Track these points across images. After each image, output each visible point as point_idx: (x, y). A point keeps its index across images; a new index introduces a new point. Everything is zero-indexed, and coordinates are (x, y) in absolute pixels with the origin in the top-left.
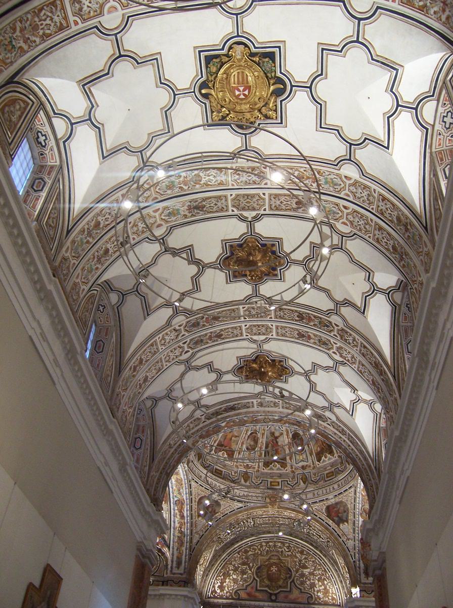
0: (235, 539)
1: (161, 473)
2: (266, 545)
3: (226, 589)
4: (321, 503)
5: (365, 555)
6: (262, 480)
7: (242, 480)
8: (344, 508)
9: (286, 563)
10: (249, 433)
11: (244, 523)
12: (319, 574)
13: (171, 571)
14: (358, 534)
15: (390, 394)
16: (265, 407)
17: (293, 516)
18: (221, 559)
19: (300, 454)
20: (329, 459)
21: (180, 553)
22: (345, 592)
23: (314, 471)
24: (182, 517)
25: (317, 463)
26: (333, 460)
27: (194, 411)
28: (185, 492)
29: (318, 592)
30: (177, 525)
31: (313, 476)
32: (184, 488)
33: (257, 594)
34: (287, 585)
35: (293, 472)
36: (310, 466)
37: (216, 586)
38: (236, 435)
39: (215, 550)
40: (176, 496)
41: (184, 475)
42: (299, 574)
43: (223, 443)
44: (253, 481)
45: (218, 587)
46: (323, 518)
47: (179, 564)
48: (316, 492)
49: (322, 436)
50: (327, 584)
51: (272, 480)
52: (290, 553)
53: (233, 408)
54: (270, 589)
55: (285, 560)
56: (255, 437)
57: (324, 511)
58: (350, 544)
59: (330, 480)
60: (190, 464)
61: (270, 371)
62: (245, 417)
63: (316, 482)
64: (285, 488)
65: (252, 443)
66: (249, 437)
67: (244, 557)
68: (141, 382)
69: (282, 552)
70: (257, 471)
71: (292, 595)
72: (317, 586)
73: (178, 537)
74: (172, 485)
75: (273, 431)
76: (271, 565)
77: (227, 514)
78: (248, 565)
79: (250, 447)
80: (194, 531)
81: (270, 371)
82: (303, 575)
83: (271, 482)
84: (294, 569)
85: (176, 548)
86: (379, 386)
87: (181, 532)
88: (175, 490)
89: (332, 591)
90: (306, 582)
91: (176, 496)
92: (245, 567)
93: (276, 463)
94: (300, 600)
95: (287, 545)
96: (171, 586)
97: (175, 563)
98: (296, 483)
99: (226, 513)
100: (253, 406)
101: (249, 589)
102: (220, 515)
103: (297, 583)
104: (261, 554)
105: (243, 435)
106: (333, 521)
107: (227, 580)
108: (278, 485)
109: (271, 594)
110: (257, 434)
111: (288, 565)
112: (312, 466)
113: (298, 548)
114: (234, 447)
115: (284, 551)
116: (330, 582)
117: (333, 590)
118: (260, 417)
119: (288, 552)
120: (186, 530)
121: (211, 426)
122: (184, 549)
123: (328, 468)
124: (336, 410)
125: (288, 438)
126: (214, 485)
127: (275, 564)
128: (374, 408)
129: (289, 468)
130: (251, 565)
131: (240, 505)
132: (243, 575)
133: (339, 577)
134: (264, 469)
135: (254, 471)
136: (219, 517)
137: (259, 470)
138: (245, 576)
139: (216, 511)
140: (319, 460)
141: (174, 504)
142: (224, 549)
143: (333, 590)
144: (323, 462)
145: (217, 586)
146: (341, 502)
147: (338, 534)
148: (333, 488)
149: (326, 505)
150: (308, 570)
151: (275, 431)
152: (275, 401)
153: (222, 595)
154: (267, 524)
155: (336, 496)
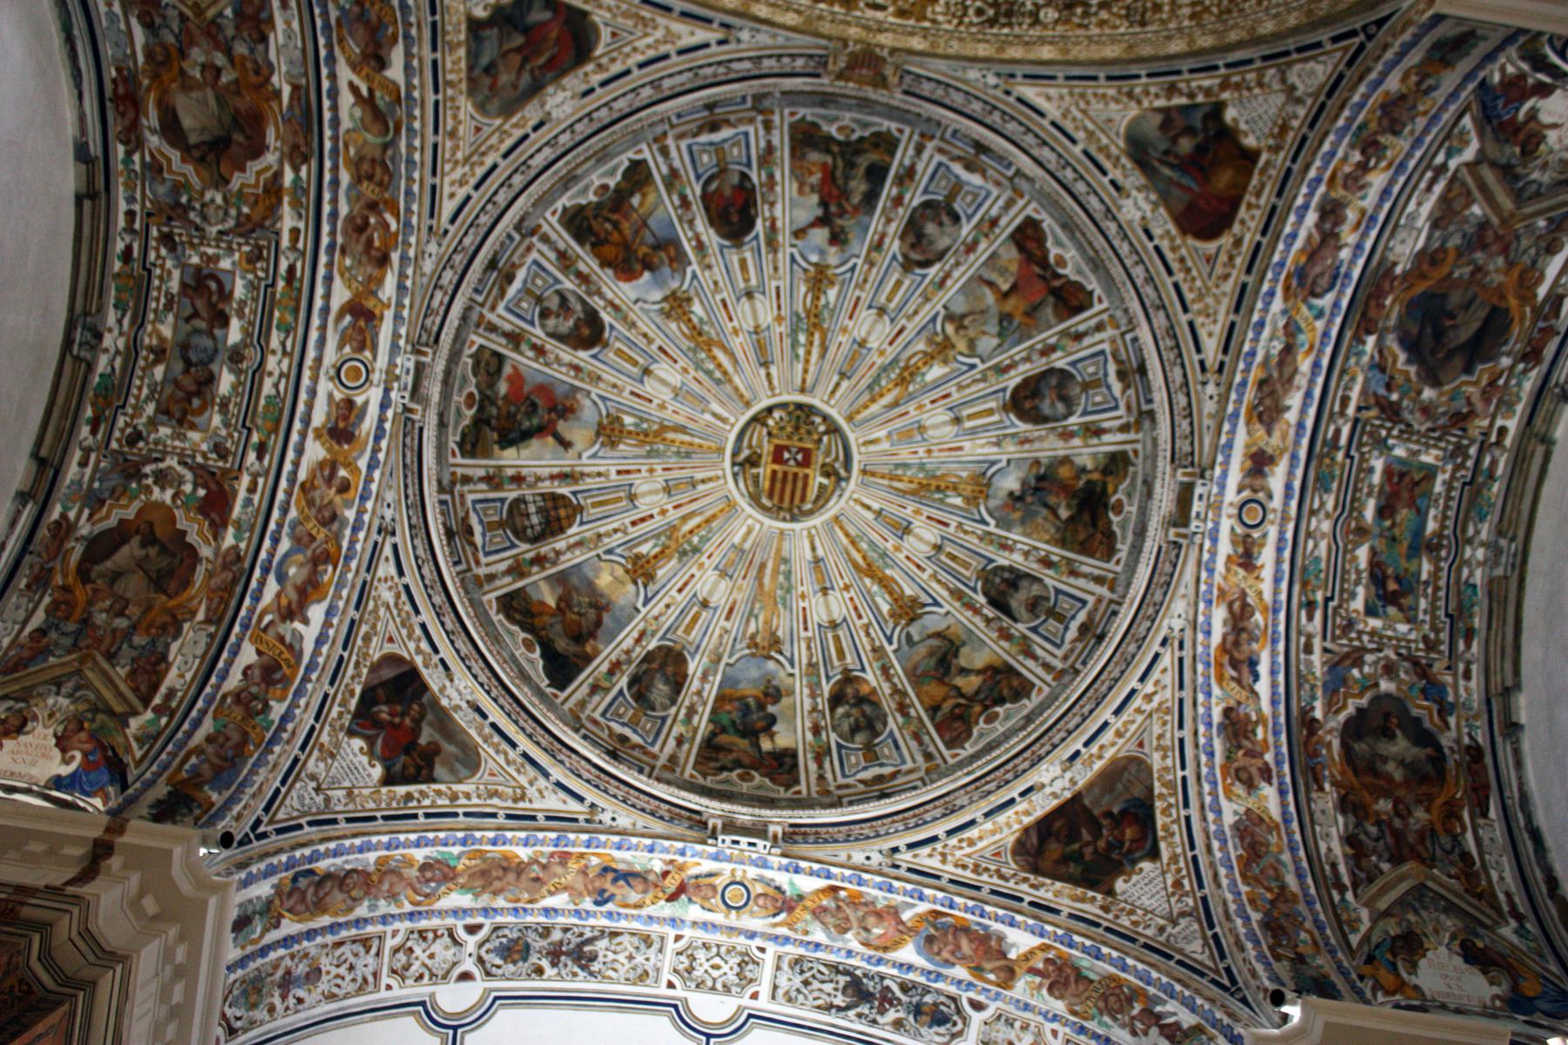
4: (617, 68)
8: (492, 87)
24: (1331, 212)
25: (647, 155)
30: (1377, 180)
32: (1259, 358)
35: (761, 112)
38: (987, 291)
41: (1229, 445)
43: (1051, 300)
56: (913, 246)
57: (605, 35)
62: (818, 946)
65: (930, 228)
66: (941, 256)
74: (1312, 382)
75: (833, 250)
77: (1109, 78)
79: (945, 219)
80: (1302, 112)
87: (1370, 147)
88: (1311, 347)
91: (1320, 314)
93: (840, 137)
105: (961, 276)
110: (905, 256)
114: (1011, 255)
120: (1339, 150)
125: (773, 220)
131: (1030, 92)
137: (922, 135)
139: (1157, 119)
141: (1347, 276)
146: (508, 110)
149: (590, 67)
151: (825, 246)
155: (536, 129)
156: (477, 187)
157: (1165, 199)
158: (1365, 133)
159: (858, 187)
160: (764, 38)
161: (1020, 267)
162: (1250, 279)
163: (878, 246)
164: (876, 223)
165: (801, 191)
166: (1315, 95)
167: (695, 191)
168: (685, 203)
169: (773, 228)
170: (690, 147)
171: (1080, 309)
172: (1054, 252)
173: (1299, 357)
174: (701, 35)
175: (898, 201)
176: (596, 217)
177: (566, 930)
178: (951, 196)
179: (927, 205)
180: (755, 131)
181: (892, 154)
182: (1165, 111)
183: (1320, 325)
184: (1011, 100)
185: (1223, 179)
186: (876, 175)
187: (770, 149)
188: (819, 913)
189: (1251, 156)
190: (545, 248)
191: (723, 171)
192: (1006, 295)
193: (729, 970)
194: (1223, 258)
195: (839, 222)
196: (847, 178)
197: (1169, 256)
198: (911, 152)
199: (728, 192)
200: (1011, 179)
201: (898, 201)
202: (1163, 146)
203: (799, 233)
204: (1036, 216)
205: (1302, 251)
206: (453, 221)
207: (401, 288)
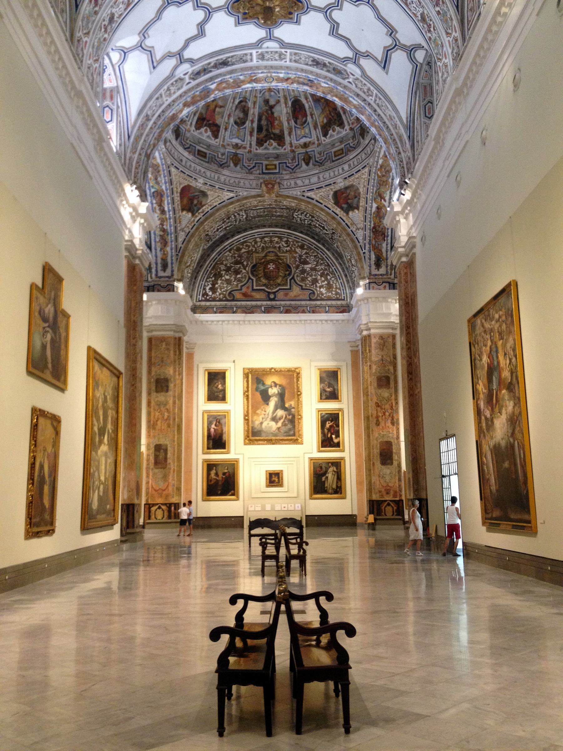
0: (225, 235)
1: (140, 154)
2: (261, 241)
3: (219, 290)
4: (328, 189)
5: (377, 245)
6: (256, 163)
7: (232, 165)
8: (355, 193)
9: (285, 260)
10: (237, 101)
11: (235, 216)
12: (322, 269)
13: (156, 275)
14: (370, 222)
15: (447, 33)
16: (268, 60)
17: (293, 205)
18: (210, 259)
19: (302, 127)
20: (339, 133)
21: (164, 254)
22: (350, 286)
23: (319, 149)
24: (163, 212)
25: (323, 138)
26: (344, 133)
27: (176, 68)
28: (163, 181)
29: (320, 287)
31: (317, 155)
32: (162, 176)
33: (254, 294)
34: (287, 283)
36: (314, 143)
37: (208, 288)
39: (204, 249)
40: (152, 187)
41: (161, 159)
42: (300, 271)
43: (204, 116)
44: (244, 164)
45: (210, 289)
46: (329, 206)
47: (165, 267)
48: (321, 176)
49: (340, 99)
50: (331, 279)
51: (267, 163)
52: (288, 248)
53: (225, 63)
54: (267, 287)
55: (284, 256)
56: (245, 106)
58: (360, 234)
59: (339, 159)
60: (168, 144)
61: (278, 5)
62: (241, 75)
63: (320, 164)
64: (284, 172)
65: (241, 115)
66: (237, 107)
67: (236, 255)
68: (106, 23)
69: (279, 247)
70: (248, 152)
71: (292, 293)
72: (320, 282)
73: (160, 236)
75: (267, 97)
76: (269, 262)
77: (216, 206)
78: (242, 263)
79: (238, 121)
80: (179, 228)
81: (278, 5)
82: (303, 271)
83: (266, 165)
84: (294, 265)
85: (158, 249)
86: (431, 23)
89: (336, 285)
90: (307, 278)
91: (152, 187)
92: (238, 266)
93: (271, 141)
94: (301, 297)
95: (285, 239)
96: (159, 291)
97: (159, 266)
98: (297, 166)
99: (215, 204)
100: (251, 60)
101: (244, 289)
102: (208, 208)
103: (298, 279)
104: (256, 252)
106: (342, 208)
107: (219, 282)
108: (275, 168)
109: (269, 293)
110: (246, 102)
111: (287, 261)
112: (316, 142)
113: (297, 242)
114: (219, 121)
115: (281, 246)
116: (333, 277)
117: (337, 284)
118: (261, 75)
119: (287, 247)
121: (198, 89)
122: (168, 249)
123: (336, 145)
124: (363, 62)
126: (198, 171)
127: (272, 261)
128: (415, 58)
129: (288, 147)
130: (245, 263)
131: (232, 195)
132: (237, 274)
133: (344, 271)
134: (256, 149)
135: (245, 152)
136: (207, 210)
138: (239, 276)
139: (203, 204)
140: (325, 135)
141: (151, 197)
142: (212, 248)
143: (337, 284)
144: (330, 137)
145: (208, 288)
146: (352, 186)
147: (346, 224)
148: (343, 169)
149: (334, 190)
150: (310, 266)
152: (281, 52)
153: (215, 297)
154: (261, 216)
155: (346, 178)
156: (360, 170)
157: (195, 188)
158: (166, 234)
159: (264, 122)
160: (295, 193)
161: (215, 120)
162: (171, 187)
163: (255, 103)
164: (257, 111)
165: (280, 118)
166: (178, 234)
167: (309, 119)
168: (312, 115)
169: (286, 103)
170: (311, 138)
171: (197, 123)
172: (209, 133)
173: (152, 178)
174: (309, 194)
175: (252, 121)
176: (335, 120)
177: (322, 69)
178: (238, 130)
179: (244, 123)
180: (295, 142)
181: (257, 139)
182: (202, 206)
183: (151, 185)
184: (235, 191)
185: (185, 201)
186: (260, 129)
187: (290, 134)
188: (243, 82)
189: (183, 210)
190: (349, 120)
191: (302, 125)
192: (216, 107)
193: (267, 56)
194: (178, 187)
195: (267, 108)
196: (267, 125)
197: (189, 179)
198: (252, 143)
199: (300, 117)
200: (226, 149)
201: (252, 121)
202: (200, 198)
203: (278, 102)
204: (217, 140)
205: (164, 201)
206: (365, 166)
207: (377, 162)
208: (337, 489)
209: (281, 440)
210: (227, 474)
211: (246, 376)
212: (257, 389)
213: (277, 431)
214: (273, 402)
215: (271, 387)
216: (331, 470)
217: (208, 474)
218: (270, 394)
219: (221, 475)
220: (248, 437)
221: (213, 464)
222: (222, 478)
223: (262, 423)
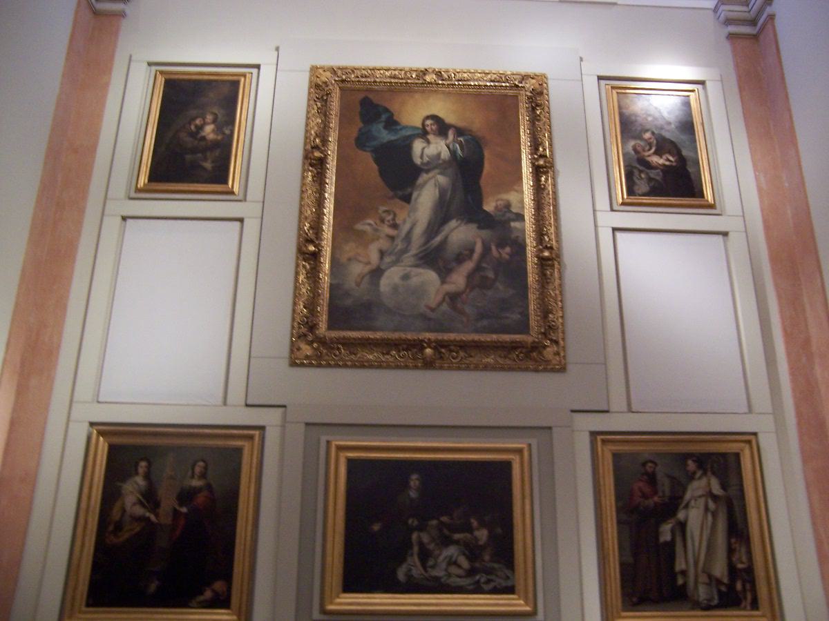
208: (731, 587)
209: (463, 346)
210: (201, 499)
211: (319, 92)
212: (362, 141)
213: (445, 307)
214: (426, 197)
215: (423, 134)
216: (696, 488)
217: (111, 494)
218: (418, 161)
219: (168, 502)
220: (312, 328)
221: (136, 448)
222: (176, 513)
223: (377, 273)
